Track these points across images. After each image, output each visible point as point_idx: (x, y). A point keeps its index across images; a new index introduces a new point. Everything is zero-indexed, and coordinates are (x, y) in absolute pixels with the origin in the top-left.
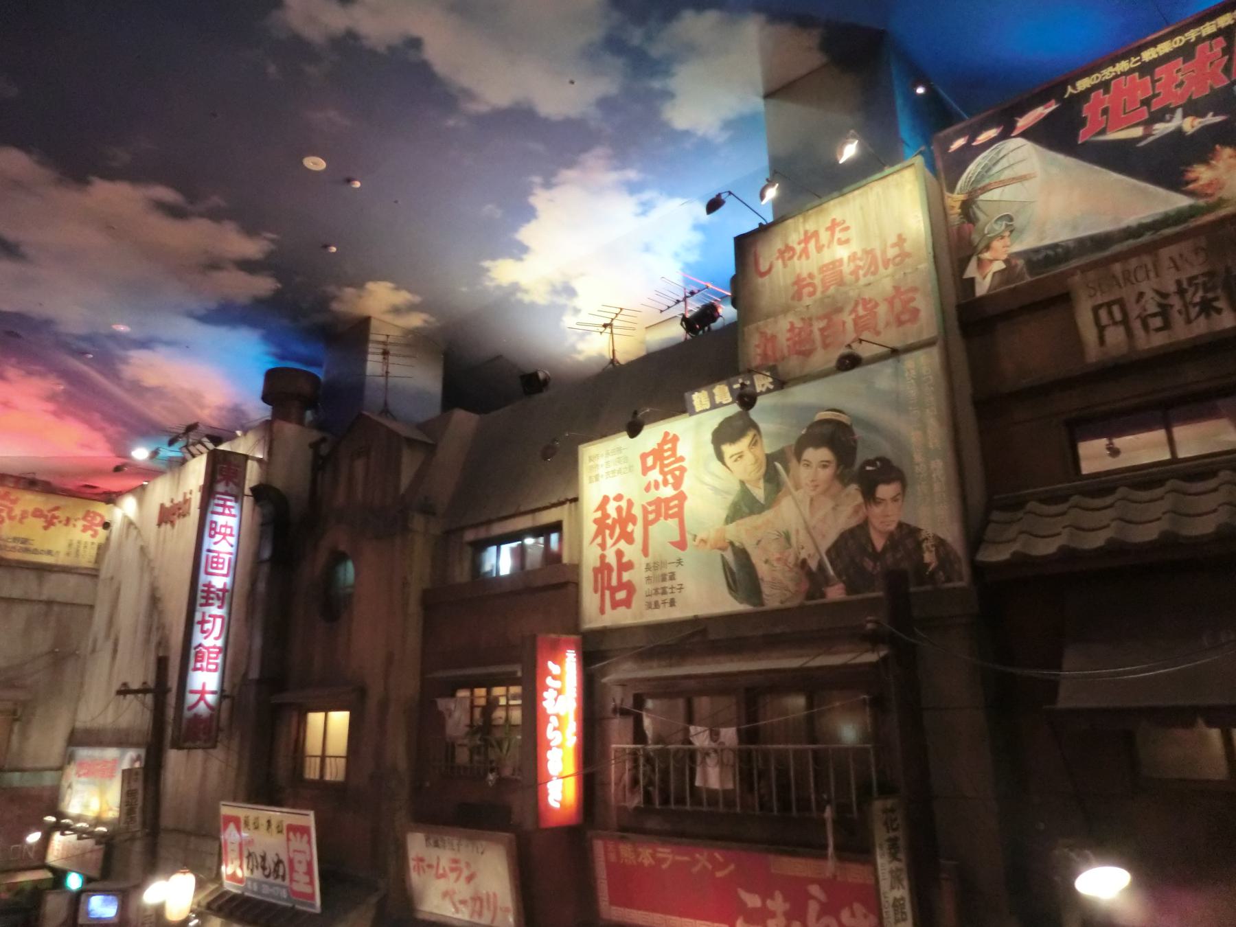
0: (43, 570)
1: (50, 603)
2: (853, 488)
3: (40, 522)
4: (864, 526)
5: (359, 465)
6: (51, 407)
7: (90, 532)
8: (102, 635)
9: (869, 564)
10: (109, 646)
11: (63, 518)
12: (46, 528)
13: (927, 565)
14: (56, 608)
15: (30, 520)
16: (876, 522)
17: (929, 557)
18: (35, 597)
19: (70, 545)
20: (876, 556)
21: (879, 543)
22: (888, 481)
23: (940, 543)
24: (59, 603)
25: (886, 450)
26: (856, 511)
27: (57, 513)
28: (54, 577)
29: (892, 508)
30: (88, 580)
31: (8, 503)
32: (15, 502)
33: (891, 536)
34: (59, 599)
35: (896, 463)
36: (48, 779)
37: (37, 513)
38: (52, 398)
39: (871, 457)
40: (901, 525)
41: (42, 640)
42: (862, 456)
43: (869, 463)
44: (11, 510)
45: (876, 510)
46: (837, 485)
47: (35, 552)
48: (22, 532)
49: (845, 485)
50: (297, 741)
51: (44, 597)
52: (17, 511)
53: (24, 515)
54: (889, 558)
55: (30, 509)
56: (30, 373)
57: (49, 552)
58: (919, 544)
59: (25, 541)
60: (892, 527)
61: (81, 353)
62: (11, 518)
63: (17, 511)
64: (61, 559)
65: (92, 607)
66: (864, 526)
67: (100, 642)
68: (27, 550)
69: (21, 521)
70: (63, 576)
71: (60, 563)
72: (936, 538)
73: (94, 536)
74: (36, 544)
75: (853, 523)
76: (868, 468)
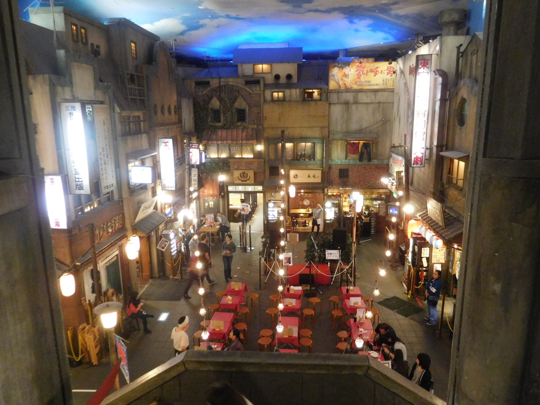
0: (376, 91)
1: (379, 103)
3: (373, 74)
5: (474, 57)
6: (370, 28)
7: (390, 75)
8: (396, 115)
10: (398, 119)
11: (380, 71)
12: (375, 76)
14: (381, 104)
15: (370, 74)
18: (374, 101)
19: (383, 81)
24: (383, 103)
27: (378, 69)
28: (380, 93)
30: (391, 93)
31: (361, 69)
32: (364, 68)
34: (382, 101)
36: (385, 162)
37: (372, 71)
38: (369, 26)
41: (379, 117)
44: (363, 71)
47: (372, 85)
48: (367, 78)
50: (450, 169)
51: (377, 101)
52: (365, 72)
53: (367, 73)
55: (369, 70)
56: (361, 19)
57: (377, 85)
59: (369, 82)
61: (374, 11)
62: (364, 74)
63: (365, 72)
64: (381, 87)
65: (393, 103)
67: (396, 115)
68: (370, 85)
69: (367, 75)
70: (383, 93)
71: (381, 88)
73: (391, 76)
74: (373, 83)
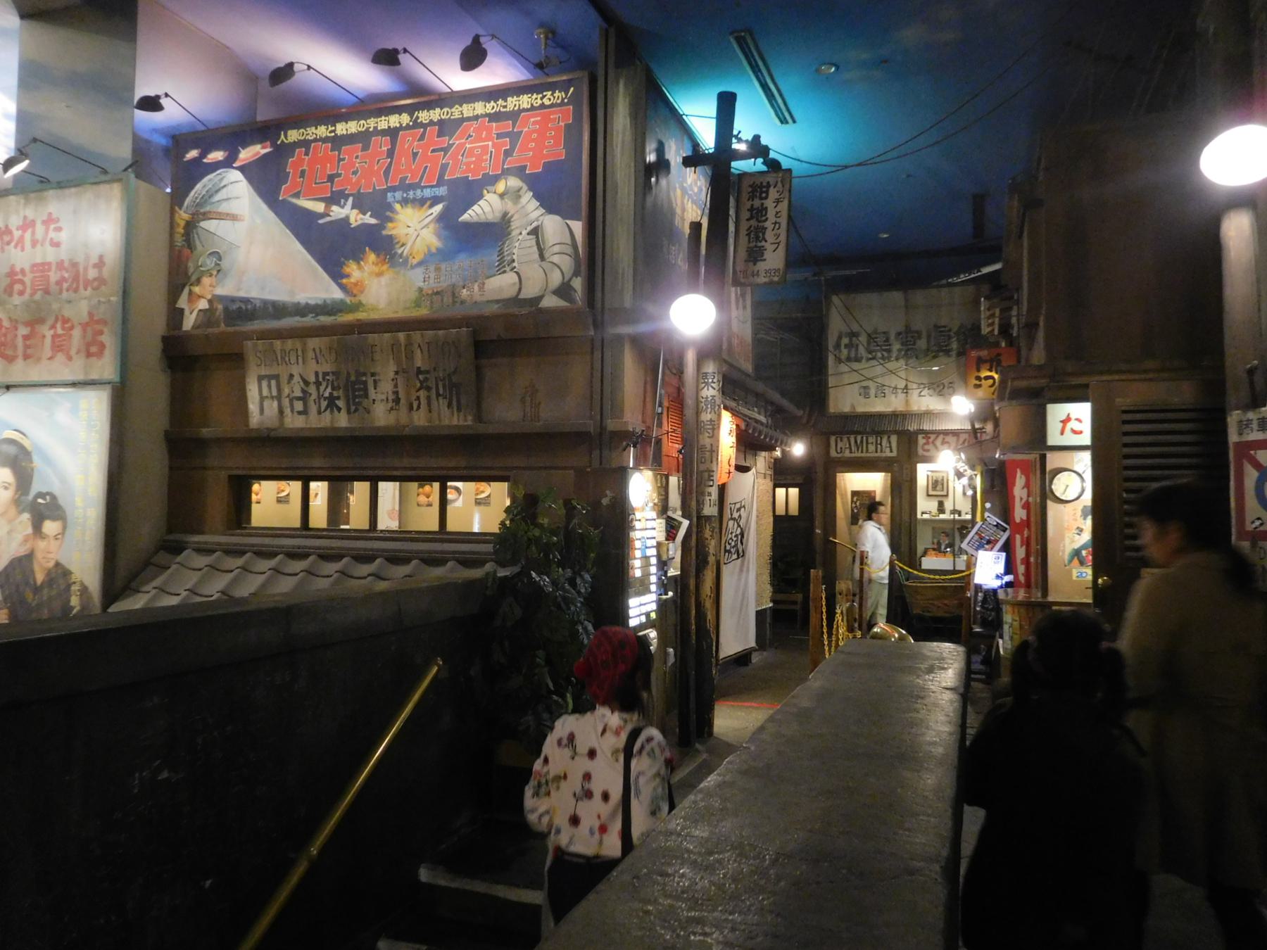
2: (26, 516)
4: (30, 556)
9: (29, 596)
13: (73, 608)
16: (39, 555)
17: (75, 601)
20: (37, 590)
21: (40, 577)
22: (54, 519)
23: (84, 590)
25: (56, 489)
26: (26, 540)
29: (54, 545)
33: (49, 573)
35: (61, 502)
39: (44, 491)
40: (57, 564)
42: (36, 487)
43: (41, 495)
45: (41, 545)
46: (13, 511)
49: (21, 512)
54: (45, 591)
58: (69, 586)
60: (51, 564)
66: (30, 556)
72: (82, 584)
75: (22, 551)
76: (40, 501)
